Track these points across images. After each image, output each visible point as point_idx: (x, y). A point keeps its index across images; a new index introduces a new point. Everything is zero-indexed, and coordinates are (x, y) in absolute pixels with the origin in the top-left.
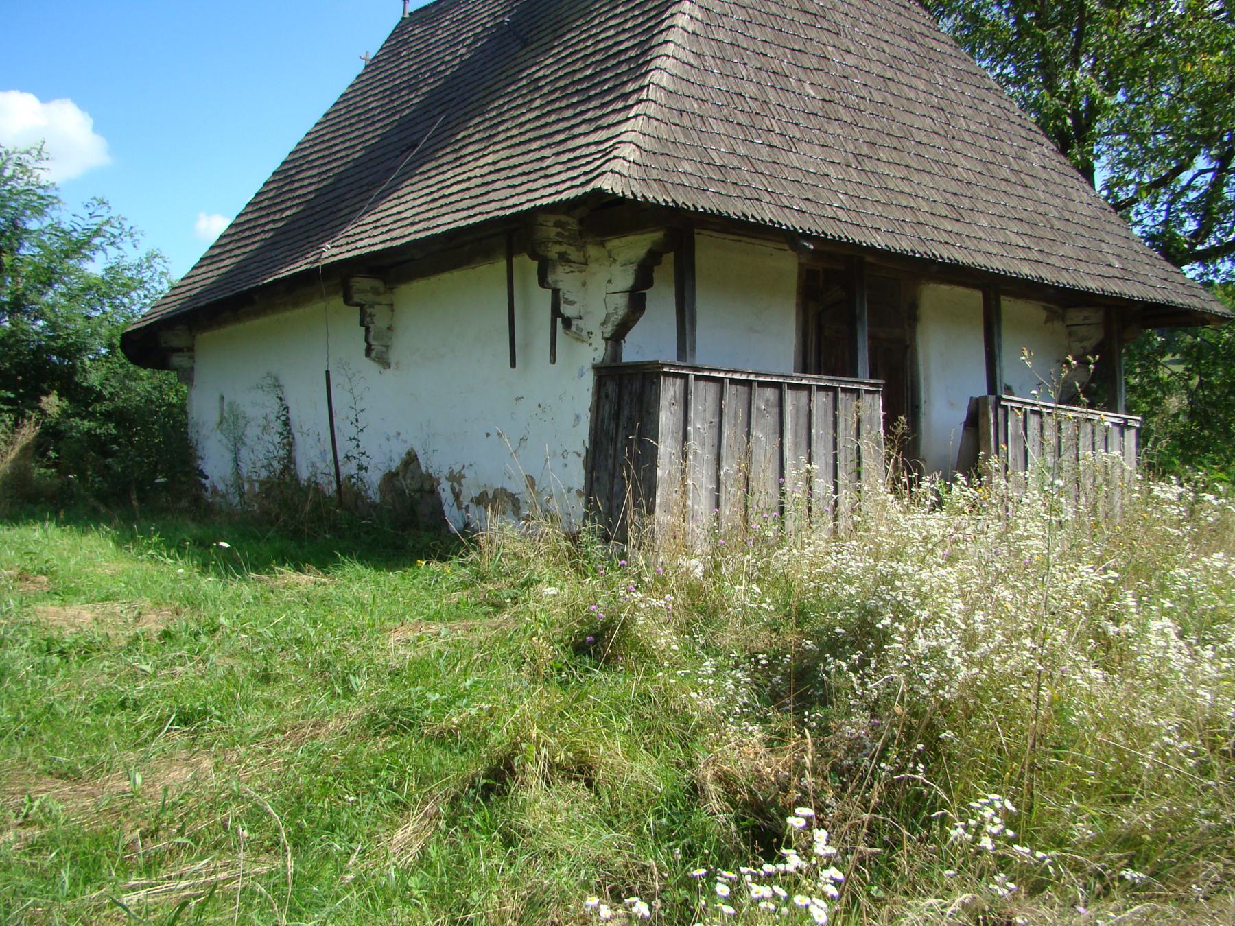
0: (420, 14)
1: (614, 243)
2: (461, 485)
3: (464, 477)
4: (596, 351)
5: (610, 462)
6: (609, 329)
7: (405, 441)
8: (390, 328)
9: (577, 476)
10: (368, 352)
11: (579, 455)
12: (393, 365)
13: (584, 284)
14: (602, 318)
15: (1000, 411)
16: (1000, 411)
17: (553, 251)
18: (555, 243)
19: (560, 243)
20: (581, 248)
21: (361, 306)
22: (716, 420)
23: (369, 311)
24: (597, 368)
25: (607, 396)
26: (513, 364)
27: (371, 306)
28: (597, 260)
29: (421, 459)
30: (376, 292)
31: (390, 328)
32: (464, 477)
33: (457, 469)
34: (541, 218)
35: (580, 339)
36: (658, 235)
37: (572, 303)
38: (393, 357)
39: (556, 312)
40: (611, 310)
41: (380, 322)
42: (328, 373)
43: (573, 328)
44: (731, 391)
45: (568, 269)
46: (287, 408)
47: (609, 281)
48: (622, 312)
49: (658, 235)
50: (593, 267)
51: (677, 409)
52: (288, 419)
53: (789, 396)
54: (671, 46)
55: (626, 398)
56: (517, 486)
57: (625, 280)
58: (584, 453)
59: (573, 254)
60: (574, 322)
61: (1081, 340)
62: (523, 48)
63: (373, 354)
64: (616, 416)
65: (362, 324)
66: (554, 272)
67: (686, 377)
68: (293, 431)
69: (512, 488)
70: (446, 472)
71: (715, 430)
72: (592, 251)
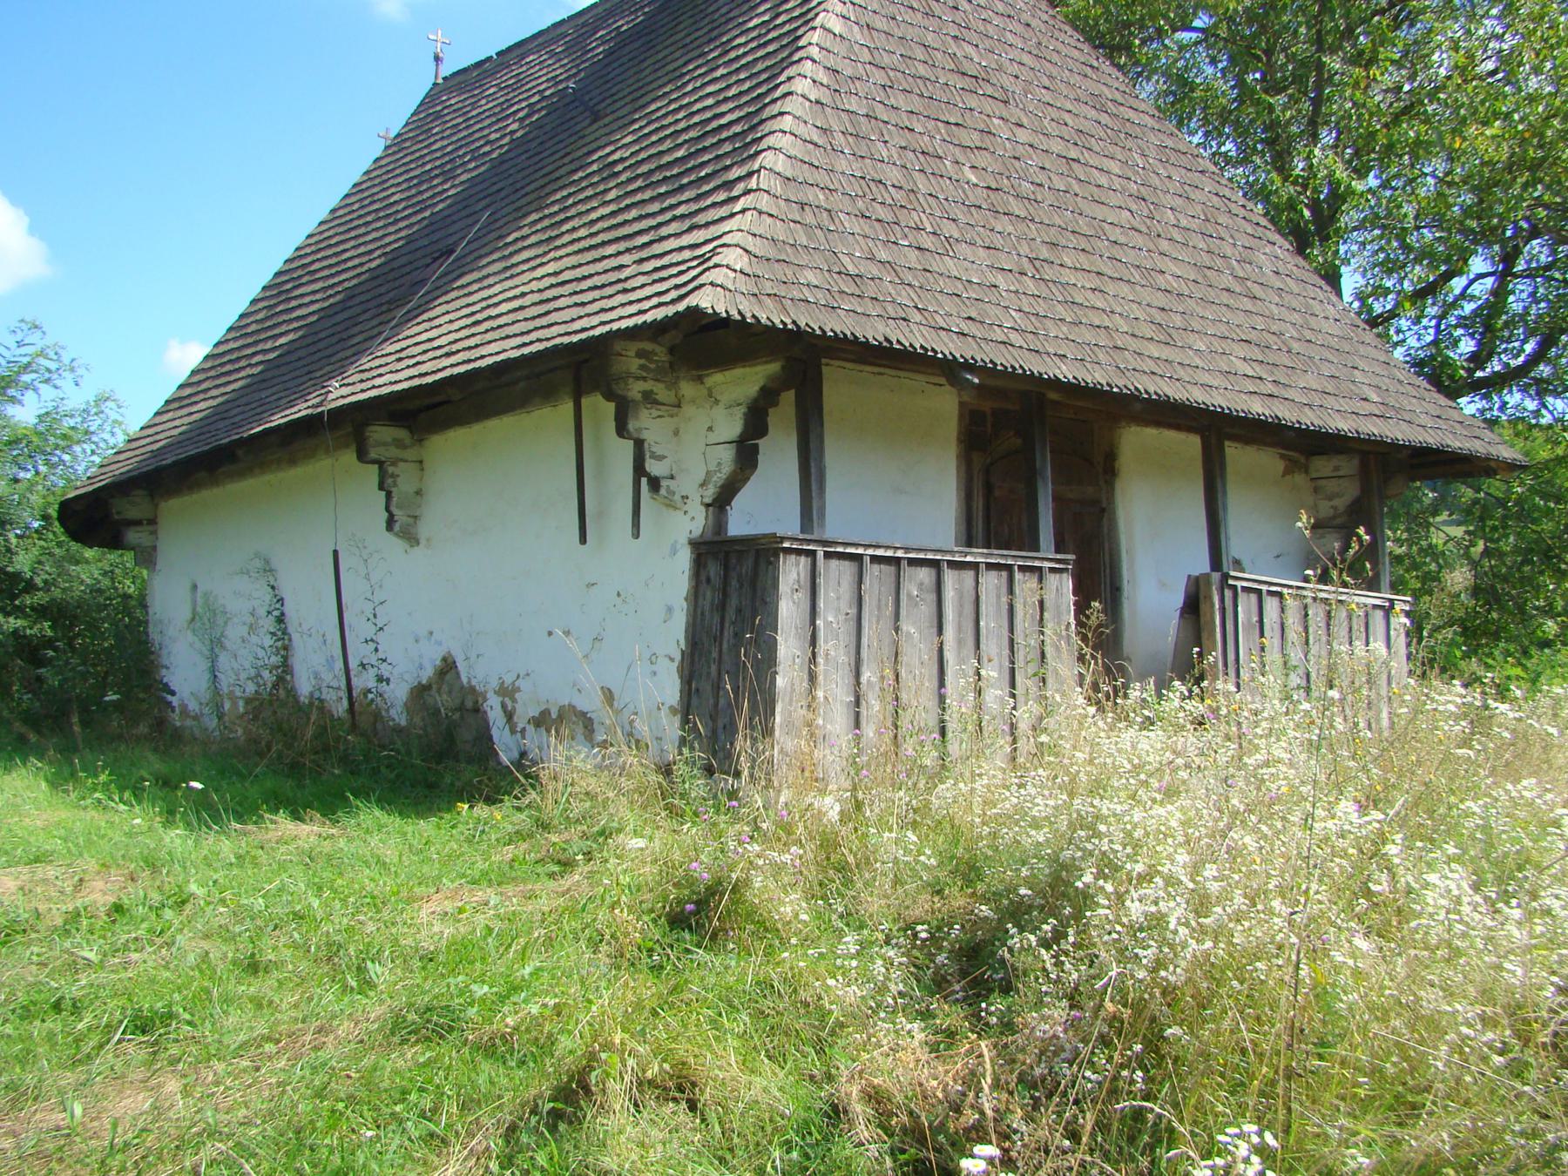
0: (459, 79)
1: (716, 378)
2: (514, 701)
3: (518, 690)
4: (693, 521)
5: (714, 668)
6: (710, 493)
7: (440, 643)
8: (419, 493)
9: (669, 689)
10: (390, 523)
11: (672, 660)
12: (423, 542)
13: (676, 433)
14: (701, 476)
15: (1228, 593)
16: (1228, 593)
17: (635, 390)
18: (637, 378)
19: (644, 379)
20: (673, 385)
21: (381, 463)
22: (854, 611)
23: (391, 469)
24: (695, 544)
25: (708, 580)
26: (583, 539)
27: (394, 464)
28: (693, 401)
29: (461, 666)
30: (399, 444)
31: (419, 493)
32: (518, 690)
33: (508, 680)
34: (618, 346)
35: (671, 506)
36: (774, 368)
37: (661, 458)
38: (423, 530)
39: (639, 470)
40: (712, 468)
41: (405, 483)
42: (336, 553)
43: (663, 491)
44: (873, 572)
45: (655, 413)
46: (281, 600)
47: (710, 429)
48: (727, 468)
49: (774, 368)
50: (688, 410)
51: (803, 597)
52: (283, 614)
53: (950, 577)
54: (788, 118)
55: (734, 583)
56: (590, 702)
57: (731, 426)
58: (678, 657)
60: (664, 483)
61: (1330, 499)
62: (594, 121)
63: (397, 527)
64: (722, 607)
65: (381, 488)
66: (637, 418)
67: (813, 553)
68: (290, 630)
69: (583, 704)
70: (495, 684)
71: (853, 624)
72: (687, 389)
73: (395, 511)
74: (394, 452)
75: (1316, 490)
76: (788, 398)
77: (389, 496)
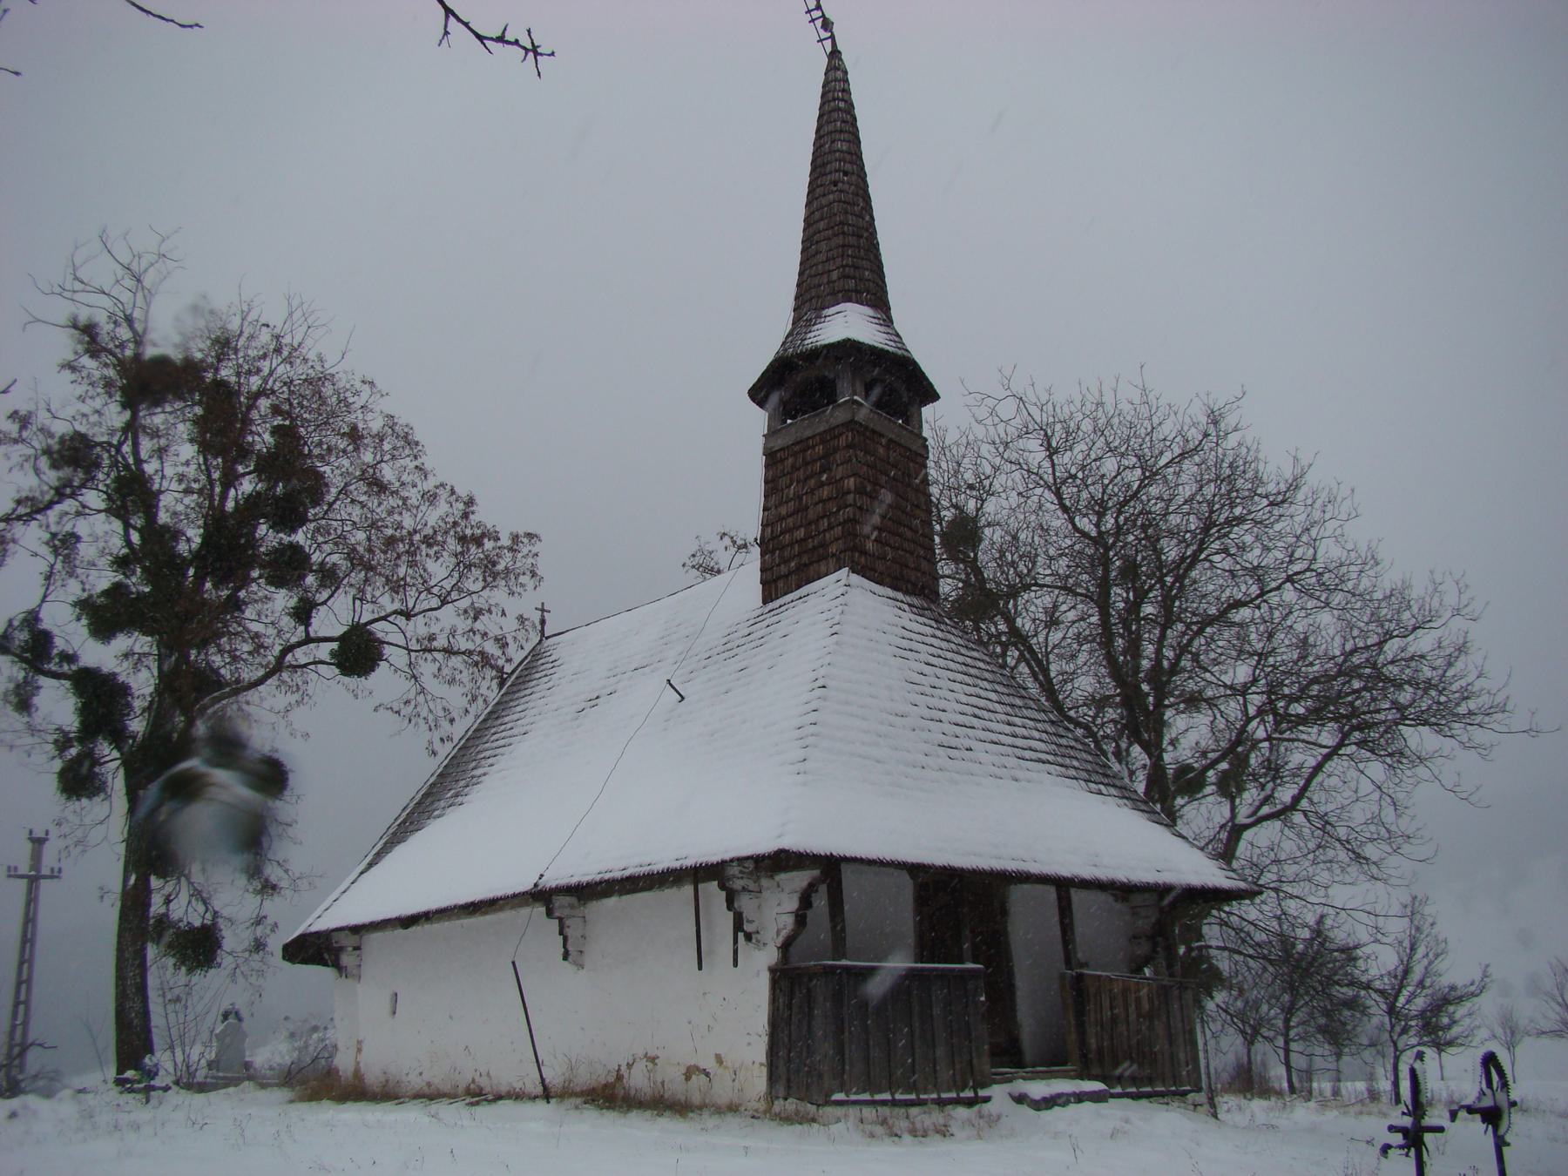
1: (782, 877)
10: (566, 956)
20: (757, 880)
24: (772, 970)
26: (700, 968)
30: (572, 907)
36: (816, 873)
39: (738, 925)
49: (816, 873)
50: (766, 894)
57: (793, 904)
59: (752, 886)
65: (561, 933)
72: (765, 882)
73: (570, 948)
74: (567, 911)
75: (1134, 914)
76: (823, 888)
77: (565, 940)
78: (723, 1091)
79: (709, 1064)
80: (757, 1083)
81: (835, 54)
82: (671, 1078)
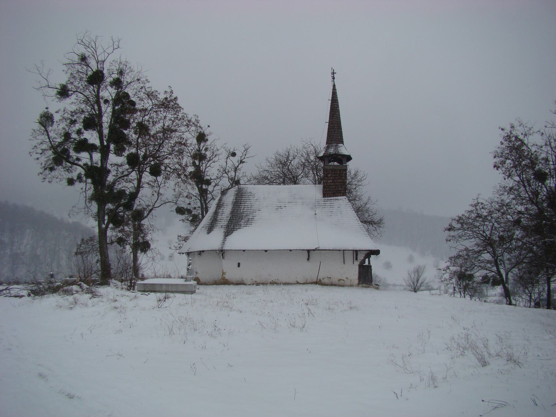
9: (357, 277)
78: (348, 282)
79: (345, 279)
80: (357, 282)
81: (334, 86)
82: (335, 281)
